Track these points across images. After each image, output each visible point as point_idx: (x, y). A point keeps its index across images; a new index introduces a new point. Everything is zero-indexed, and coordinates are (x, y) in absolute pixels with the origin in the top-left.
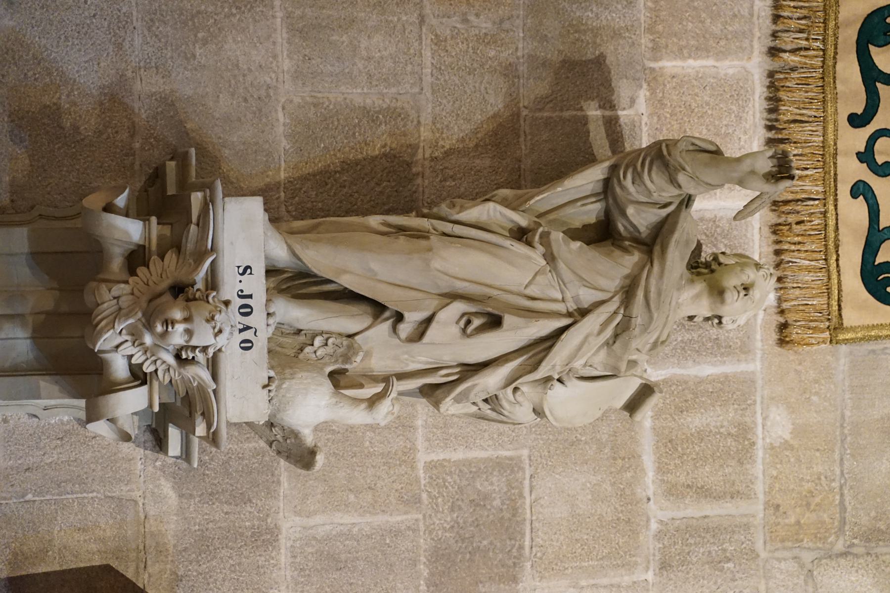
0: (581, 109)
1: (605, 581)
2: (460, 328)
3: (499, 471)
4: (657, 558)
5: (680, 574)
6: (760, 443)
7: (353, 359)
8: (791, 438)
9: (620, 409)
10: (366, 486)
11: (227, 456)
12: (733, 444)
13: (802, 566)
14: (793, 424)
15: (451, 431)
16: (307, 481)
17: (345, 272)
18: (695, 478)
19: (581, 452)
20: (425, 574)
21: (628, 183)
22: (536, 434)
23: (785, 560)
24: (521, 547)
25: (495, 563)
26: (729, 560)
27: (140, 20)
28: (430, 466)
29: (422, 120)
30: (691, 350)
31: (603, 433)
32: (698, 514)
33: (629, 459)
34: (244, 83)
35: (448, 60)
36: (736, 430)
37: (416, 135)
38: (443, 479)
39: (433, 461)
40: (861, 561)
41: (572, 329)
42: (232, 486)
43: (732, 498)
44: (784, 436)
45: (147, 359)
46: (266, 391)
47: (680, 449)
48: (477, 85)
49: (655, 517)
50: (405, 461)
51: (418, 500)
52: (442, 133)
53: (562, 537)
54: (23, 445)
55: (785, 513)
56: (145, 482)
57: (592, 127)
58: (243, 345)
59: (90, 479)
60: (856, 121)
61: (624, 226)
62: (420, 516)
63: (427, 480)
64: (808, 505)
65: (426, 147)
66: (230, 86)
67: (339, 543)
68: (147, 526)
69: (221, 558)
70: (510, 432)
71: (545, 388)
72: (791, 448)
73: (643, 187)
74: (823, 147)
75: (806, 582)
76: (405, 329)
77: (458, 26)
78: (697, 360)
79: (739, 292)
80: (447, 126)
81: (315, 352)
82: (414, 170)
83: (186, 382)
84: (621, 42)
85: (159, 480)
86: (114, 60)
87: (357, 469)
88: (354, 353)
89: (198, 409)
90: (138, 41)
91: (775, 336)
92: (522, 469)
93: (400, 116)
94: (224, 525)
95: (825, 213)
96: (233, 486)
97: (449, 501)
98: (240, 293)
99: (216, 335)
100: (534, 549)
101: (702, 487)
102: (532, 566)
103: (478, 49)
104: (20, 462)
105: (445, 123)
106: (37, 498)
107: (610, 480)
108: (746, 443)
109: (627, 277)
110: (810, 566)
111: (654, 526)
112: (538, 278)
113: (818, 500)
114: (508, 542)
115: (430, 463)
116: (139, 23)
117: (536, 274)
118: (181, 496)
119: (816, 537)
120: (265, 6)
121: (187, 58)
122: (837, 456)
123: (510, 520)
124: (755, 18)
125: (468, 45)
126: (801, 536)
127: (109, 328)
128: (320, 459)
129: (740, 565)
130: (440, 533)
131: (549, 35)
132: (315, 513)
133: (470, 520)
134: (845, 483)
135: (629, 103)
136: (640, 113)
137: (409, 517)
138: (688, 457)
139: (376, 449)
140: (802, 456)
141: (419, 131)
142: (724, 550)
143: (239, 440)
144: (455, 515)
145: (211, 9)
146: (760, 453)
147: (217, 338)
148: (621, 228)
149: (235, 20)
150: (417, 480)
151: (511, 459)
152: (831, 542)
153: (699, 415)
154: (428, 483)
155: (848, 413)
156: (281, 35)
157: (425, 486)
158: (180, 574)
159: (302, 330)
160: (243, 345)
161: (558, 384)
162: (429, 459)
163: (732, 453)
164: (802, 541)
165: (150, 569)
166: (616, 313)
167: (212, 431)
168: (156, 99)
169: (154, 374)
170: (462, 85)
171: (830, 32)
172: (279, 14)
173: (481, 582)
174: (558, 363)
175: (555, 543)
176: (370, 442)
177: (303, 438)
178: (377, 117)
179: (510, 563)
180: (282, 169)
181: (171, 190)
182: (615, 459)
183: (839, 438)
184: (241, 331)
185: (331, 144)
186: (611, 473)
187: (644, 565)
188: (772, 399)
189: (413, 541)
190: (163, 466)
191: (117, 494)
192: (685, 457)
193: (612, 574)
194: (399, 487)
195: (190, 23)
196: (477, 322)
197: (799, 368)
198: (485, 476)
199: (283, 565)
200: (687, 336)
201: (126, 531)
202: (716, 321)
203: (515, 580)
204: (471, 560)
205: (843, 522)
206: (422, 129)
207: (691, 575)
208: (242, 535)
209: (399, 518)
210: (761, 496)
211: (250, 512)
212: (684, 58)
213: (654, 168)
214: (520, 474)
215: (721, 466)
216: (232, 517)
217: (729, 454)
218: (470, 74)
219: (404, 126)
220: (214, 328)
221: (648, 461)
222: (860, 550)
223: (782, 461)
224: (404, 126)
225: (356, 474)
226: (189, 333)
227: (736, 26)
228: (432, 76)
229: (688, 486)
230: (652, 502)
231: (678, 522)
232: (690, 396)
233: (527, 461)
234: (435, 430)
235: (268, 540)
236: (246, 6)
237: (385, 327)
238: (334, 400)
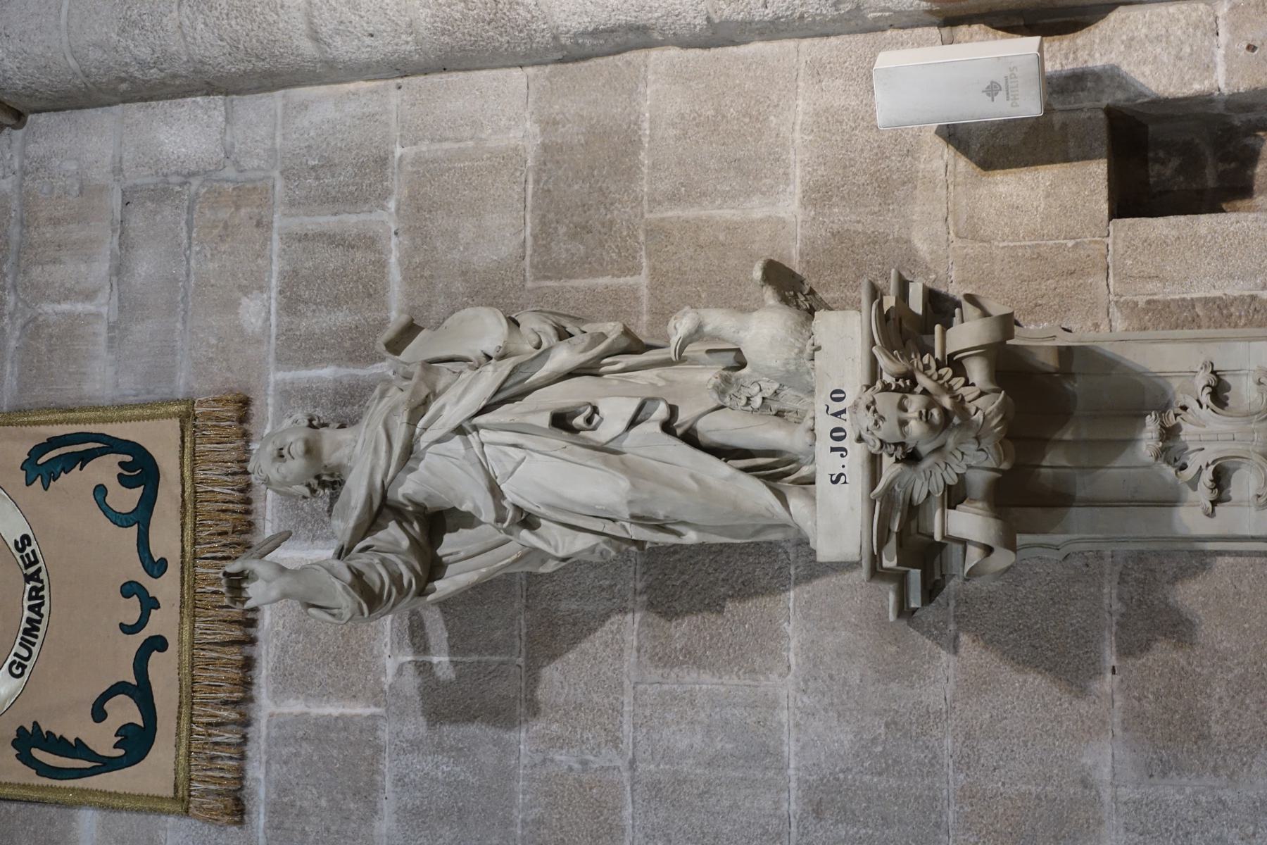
0: (455, 664)
1: (446, 145)
3: (559, 264)
4: (390, 170)
5: (367, 153)
6: (274, 294)
8: (240, 299)
9: (422, 329)
12: (302, 293)
13: (236, 163)
15: (611, 308)
20: (643, 154)
21: (407, 575)
23: (254, 169)
24: (537, 182)
25: (566, 165)
26: (313, 168)
27: (945, 765)
28: (635, 270)
29: (635, 654)
32: (344, 217)
35: (604, 720)
37: (642, 636)
39: (632, 276)
40: (173, 169)
41: (474, 411)
43: (306, 235)
48: (572, 692)
49: (390, 214)
51: (648, 233)
53: (492, 192)
54: (1077, 299)
55: (251, 218)
56: (948, 257)
57: (445, 645)
58: (842, 395)
59: (1006, 260)
60: (158, 643)
61: (413, 528)
62: (647, 216)
64: (226, 227)
66: (848, 693)
67: (737, 187)
68: (945, 210)
69: (865, 173)
71: (506, 348)
75: (233, 145)
76: (661, 412)
77: (592, 758)
81: (761, 390)
82: (645, 598)
83: (906, 355)
84: (410, 737)
86: (975, 721)
87: (715, 268)
90: (948, 742)
91: (253, 410)
92: (532, 266)
93: (660, 658)
94: (862, 210)
95: (195, 543)
97: (615, 232)
99: (873, 402)
100: (523, 180)
101: (337, 246)
102: (526, 161)
104: (1081, 281)
105: (609, 649)
106: (1062, 241)
108: (288, 294)
110: (228, 162)
111: (392, 205)
112: (510, 469)
113: (216, 232)
114: (551, 186)
115: (634, 274)
116: (946, 761)
117: (512, 473)
118: (908, 241)
119: (219, 193)
120: (807, 781)
121: (896, 723)
122: (193, 278)
123: (548, 211)
125: (582, 737)
126: (235, 193)
127: (989, 417)
128: (757, 274)
129: (301, 163)
130: (626, 198)
131: (491, 746)
132: (762, 221)
133: (592, 211)
134: (185, 250)
137: (659, 215)
142: (317, 178)
144: (609, 216)
145: (867, 778)
148: (416, 525)
149: (841, 765)
150: (649, 255)
152: (203, 187)
155: (179, 326)
156: (790, 749)
157: (641, 249)
158: (910, 158)
160: (842, 395)
161: (491, 353)
162: (636, 277)
164: (234, 189)
165: (941, 164)
168: (930, 678)
170: (590, 692)
171: (184, 742)
172: (791, 772)
173: (582, 145)
175: (500, 186)
179: (549, 165)
180: (792, 600)
181: (915, 575)
182: (432, 276)
183: (190, 299)
184: (844, 411)
185: (737, 628)
186: (436, 261)
187: (404, 162)
188: (259, 342)
189: (656, 189)
190: (928, 274)
191: (978, 245)
192: (355, 278)
193: (439, 153)
194: (669, 247)
195: (890, 762)
197: (229, 375)
199: (798, 165)
200: (348, 410)
201: (968, 205)
202: (315, 423)
203: (545, 147)
204: (592, 168)
205: (190, 210)
206: (635, 644)
207: (354, 152)
208: (843, 198)
209: (670, 214)
210: (275, 236)
211: (833, 222)
212: (341, 717)
214: (535, 262)
215: (316, 269)
216: (854, 217)
218: (581, 704)
220: (875, 411)
221: (395, 274)
222: (174, 179)
224: (655, 647)
225: (716, 262)
226: (902, 408)
227: (285, 751)
228: (622, 703)
229: (353, 248)
230: (393, 231)
231: (365, 209)
233: (528, 274)
235: (814, 192)
236: (828, 781)
237: (684, 416)
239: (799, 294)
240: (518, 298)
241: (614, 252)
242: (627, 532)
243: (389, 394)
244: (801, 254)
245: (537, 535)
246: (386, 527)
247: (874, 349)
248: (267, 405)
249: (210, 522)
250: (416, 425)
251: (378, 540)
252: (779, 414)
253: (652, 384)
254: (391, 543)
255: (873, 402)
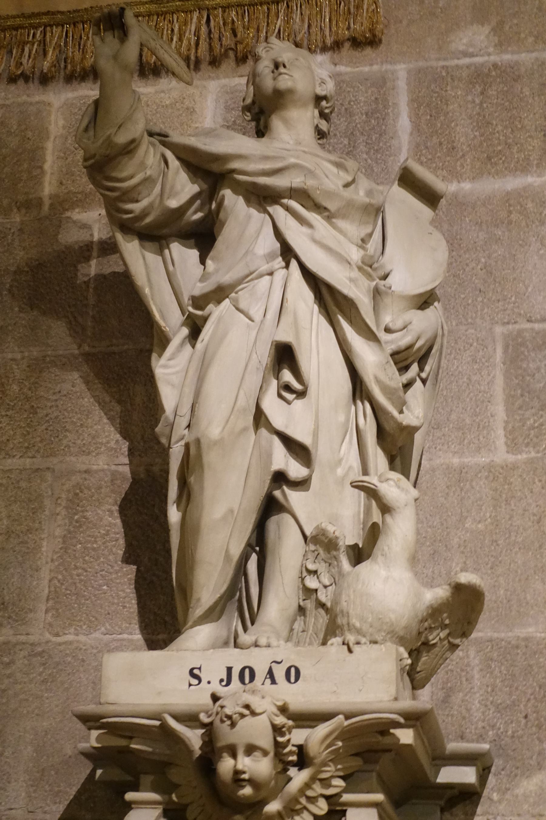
0: (87, 283)
2: (297, 398)
3: (522, 360)
7: (331, 535)
9: (434, 211)
10: (536, 527)
11: (490, 706)
12: (494, 88)
14: (472, 24)
15: (468, 421)
16: (527, 603)
17: (227, 551)
18: (536, 128)
19: (499, 262)
21: (137, 207)
22: (476, 317)
30: (379, 143)
31: (478, 237)
33: (510, 205)
34: (25, 683)
36: (477, 86)
37: (101, 474)
38: (529, 429)
39: (506, 443)
41: (304, 259)
42: (529, 700)
44: (487, 32)
45: (305, 808)
46: (356, 649)
47: (499, 148)
48: (49, 404)
50: (505, 478)
52: (101, 443)
57: (107, 271)
58: (293, 679)
61: (195, 212)
63: (531, 449)
65: (116, 463)
70: (472, 348)
71: (386, 293)
72: (501, 24)
73: (140, 188)
74: (149, 16)
78: (391, 135)
79: (280, 74)
80: (93, 438)
81: (326, 587)
85: (517, 796)
87: (513, 538)
88: (323, 535)
89: (374, 740)
91: (368, 51)
92: (520, 332)
93: (77, 494)
96: (529, 700)
98: (224, 683)
99: (254, 714)
103: (8, 405)
107: (537, 226)
109: (248, 201)
112: (242, 306)
117: (238, 309)
124: (7, 102)
128: (465, 578)
135: (85, 230)
136: (98, 217)
138: (510, 138)
139: (488, 515)
140: (511, 11)
141: (97, 472)
143: (469, 692)
146: (507, 57)
147: (258, 711)
148: (199, 215)
150: (531, 461)
151: (506, 348)
153: (458, 128)
154: (534, 447)
157: (538, 452)
159: (299, 606)
160: (293, 679)
161: (389, 280)
162: (503, 448)
163: (505, 89)
166: (287, 209)
167: (402, 720)
168: (35, 791)
169: (332, 800)
170: (48, 421)
171: (26, 22)
174: (348, 274)
176: (480, 522)
177: (440, 601)
178: (77, 521)
180: (130, 637)
182: (510, 223)
184: (274, 682)
186: (527, 226)
190: (499, 791)
192: (510, 141)
194: (539, 484)
196: (287, 376)
197: (405, 22)
198: (528, 378)
200: (362, 147)
202: (324, 103)
206: (95, 467)
213: (114, 174)
214: (527, 335)
215: (521, 100)
217: (507, 92)
218: (36, 413)
219: (89, 489)
220: (243, 716)
223: (516, 33)
224: (89, 489)
226: (250, 750)
228: (33, 457)
232: (435, 140)
233: (510, 327)
234: (466, 441)
238: (380, 559)
239: (447, 631)
240: (482, 318)
241: (535, 421)
242: (177, 442)
243: (342, 173)
244: (526, 639)
245: (182, 344)
246: (193, 183)
247: (341, 717)
248: (371, 65)
249: (246, 20)
250: (290, 198)
251: (177, 173)
252: (301, 610)
253: (340, 461)
254: (172, 187)
255: (254, 714)
